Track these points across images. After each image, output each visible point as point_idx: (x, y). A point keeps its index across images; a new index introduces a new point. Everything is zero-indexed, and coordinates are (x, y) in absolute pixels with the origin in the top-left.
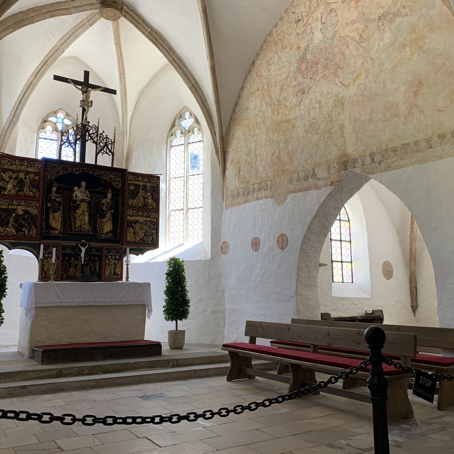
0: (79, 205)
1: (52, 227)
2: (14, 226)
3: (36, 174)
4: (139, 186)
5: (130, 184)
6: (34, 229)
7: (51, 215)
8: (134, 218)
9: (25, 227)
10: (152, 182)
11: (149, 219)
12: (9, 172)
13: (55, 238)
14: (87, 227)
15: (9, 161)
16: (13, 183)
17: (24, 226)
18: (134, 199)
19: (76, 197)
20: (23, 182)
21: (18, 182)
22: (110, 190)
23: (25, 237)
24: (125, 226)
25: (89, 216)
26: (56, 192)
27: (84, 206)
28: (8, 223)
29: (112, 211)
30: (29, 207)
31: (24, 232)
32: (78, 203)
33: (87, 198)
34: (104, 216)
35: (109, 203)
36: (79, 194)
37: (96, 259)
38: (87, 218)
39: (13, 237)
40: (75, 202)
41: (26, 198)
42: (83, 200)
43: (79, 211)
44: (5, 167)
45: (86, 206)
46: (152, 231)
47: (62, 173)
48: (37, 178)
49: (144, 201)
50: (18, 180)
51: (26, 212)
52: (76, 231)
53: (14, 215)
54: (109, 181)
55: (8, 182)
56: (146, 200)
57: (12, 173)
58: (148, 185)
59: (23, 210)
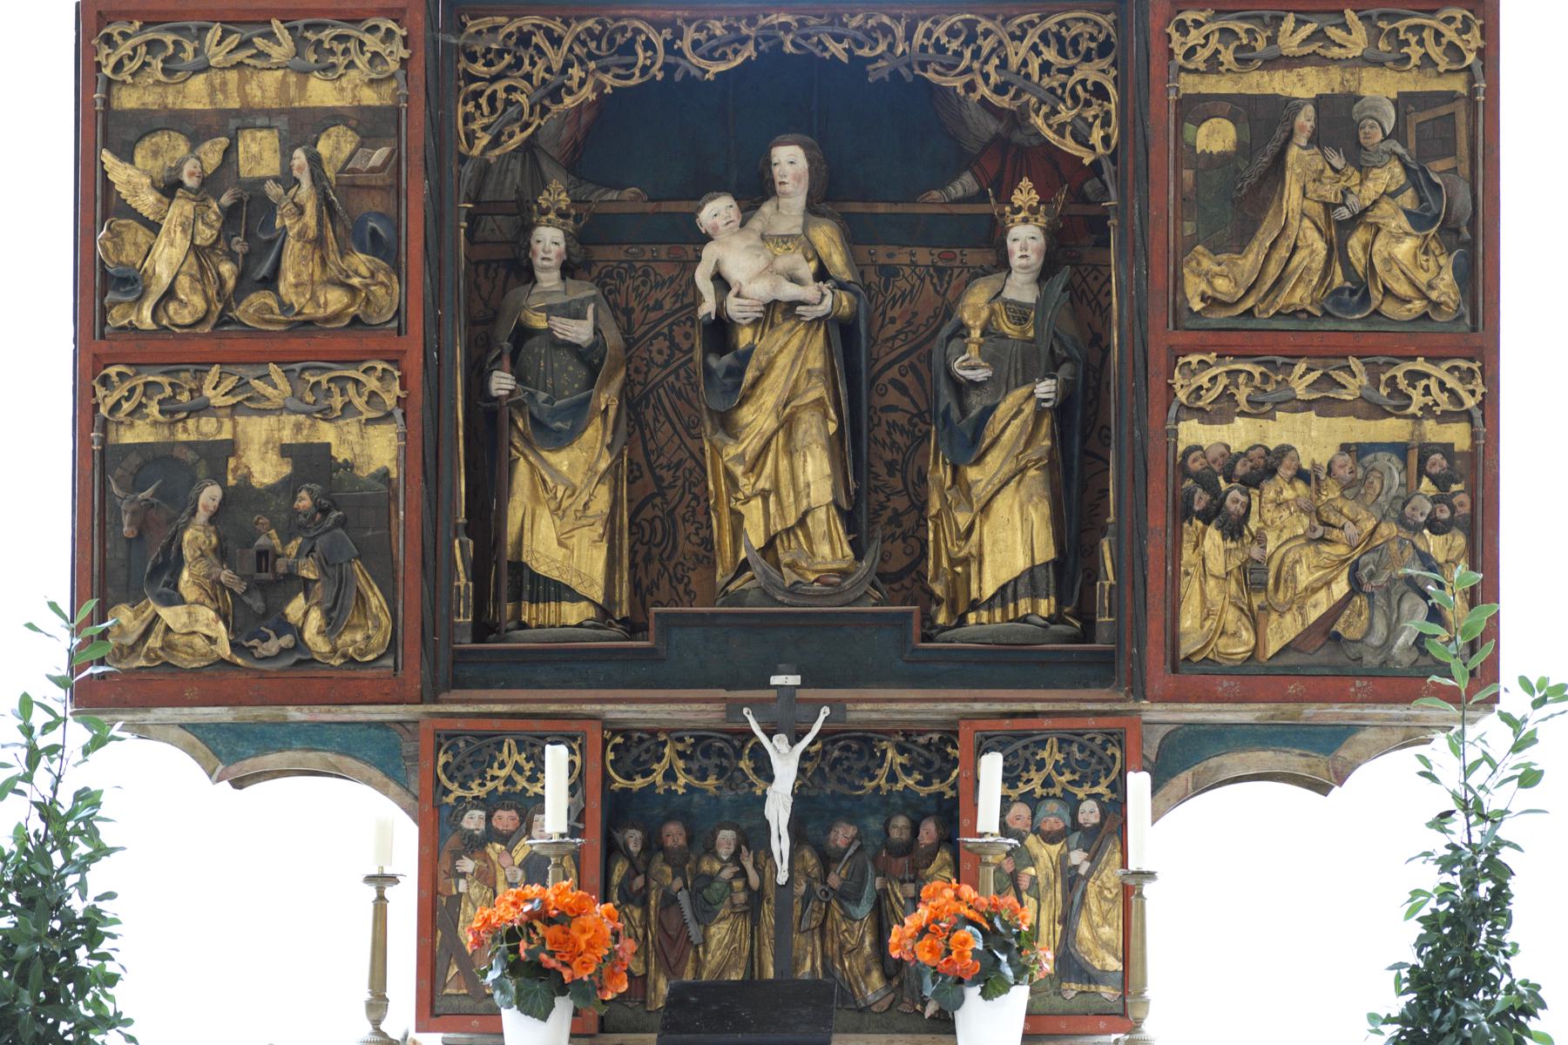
2: (214, 591)
3: (370, 125)
4: (1284, 108)
5: (1196, 109)
6: (376, 600)
8: (1239, 434)
9: (306, 586)
10: (1415, 52)
11: (1391, 429)
12: (162, 139)
13: (567, 663)
14: (828, 549)
15: (153, 46)
16: (189, 227)
17: (293, 583)
18: (1240, 242)
19: (721, 282)
20: (270, 208)
21: (230, 215)
23: (303, 676)
25: (850, 450)
27: (790, 368)
28: (171, 563)
30: (326, 414)
31: (299, 632)
34: (970, 444)
36: (756, 258)
37: (929, 832)
39: (213, 681)
41: (297, 344)
42: (776, 312)
44: (128, 100)
45: (815, 360)
46: (1435, 544)
48: (378, 156)
49: (1337, 250)
50: (226, 200)
51: (310, 462)
52: (738, 598)
53: (210, 496)
55: (154, 227)
56: (1355, 244)
57: (183, 147)
58: (1379, 87)
59: (285, 451)
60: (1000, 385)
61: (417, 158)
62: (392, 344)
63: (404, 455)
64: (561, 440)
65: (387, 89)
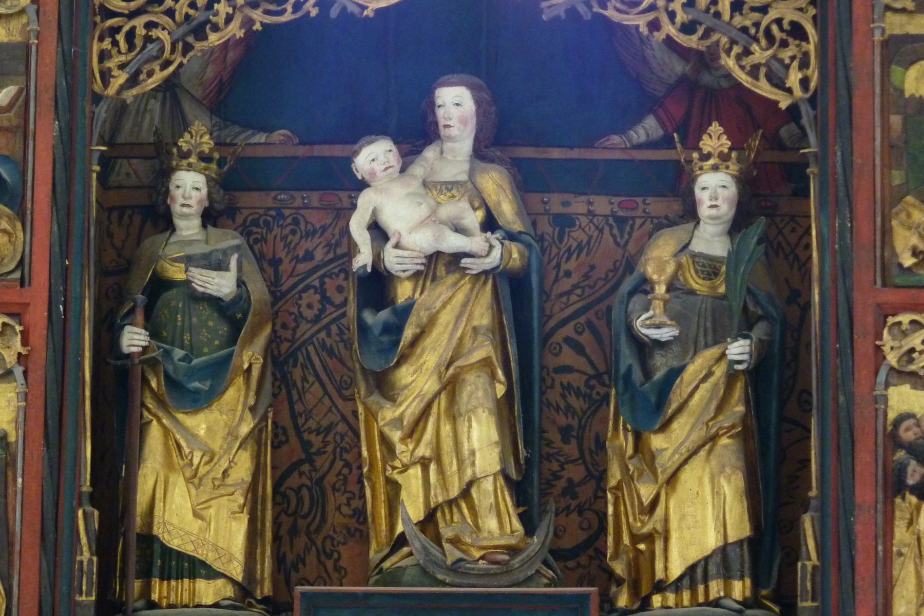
0: (405, 312)
1: (167, 552)
7: (155, 434)
14: (495, 522)
19: (378, 231)
22: (715, 140)
24: (866, 493)
25: (521, 414)
26: (209, 217)
27: (453, 328)
29: (738, 350)
32: (404, 292)
33: (476, 242)
35: (709, 267)
38: (481, 440)
40: (377, 285)
43: (417, 379)
45: (482, 316)
47: (235, 30)
52: (394, 577)
54: (692, 41)
60: (688, 344)
61: (47, 98)
62: (14, 296)
63: (25, 416)
64: (198, 401)
65: (16, 25)
